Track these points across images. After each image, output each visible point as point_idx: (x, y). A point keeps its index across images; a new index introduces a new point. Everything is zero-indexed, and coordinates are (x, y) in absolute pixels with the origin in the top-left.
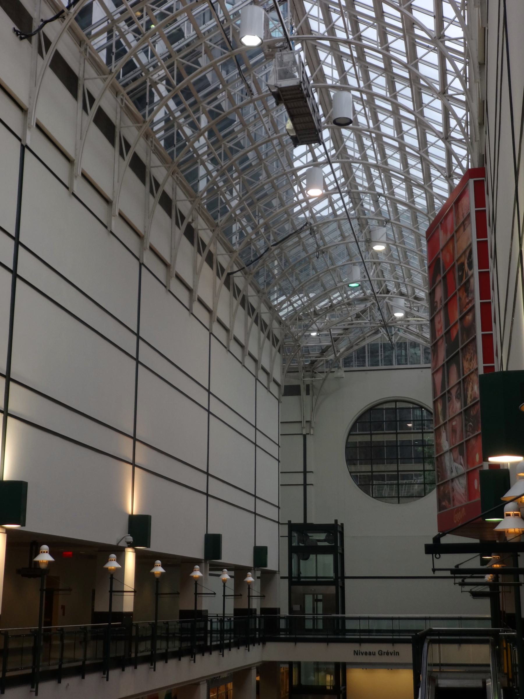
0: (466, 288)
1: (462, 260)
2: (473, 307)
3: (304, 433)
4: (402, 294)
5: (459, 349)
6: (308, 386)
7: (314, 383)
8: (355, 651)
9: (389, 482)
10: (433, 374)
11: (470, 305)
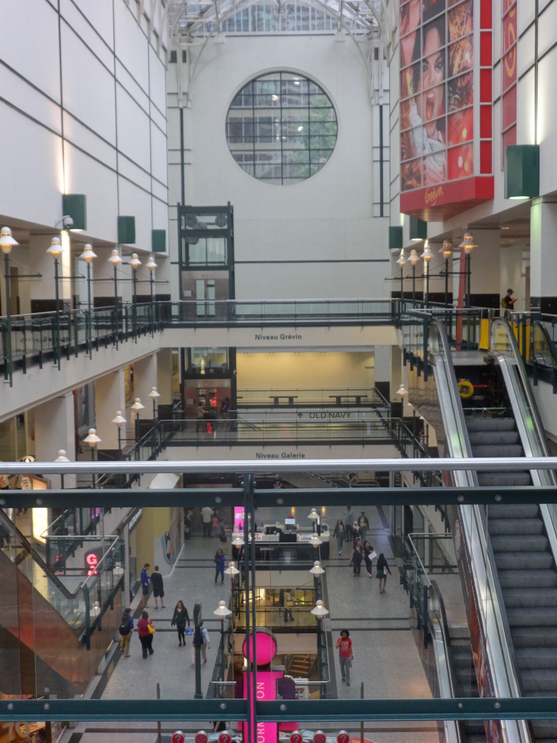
3: (181, 106)
5: (445, 11)
6: (184, 53)
7: (191, 50)
8: (256, 336)
9: (246, 162)
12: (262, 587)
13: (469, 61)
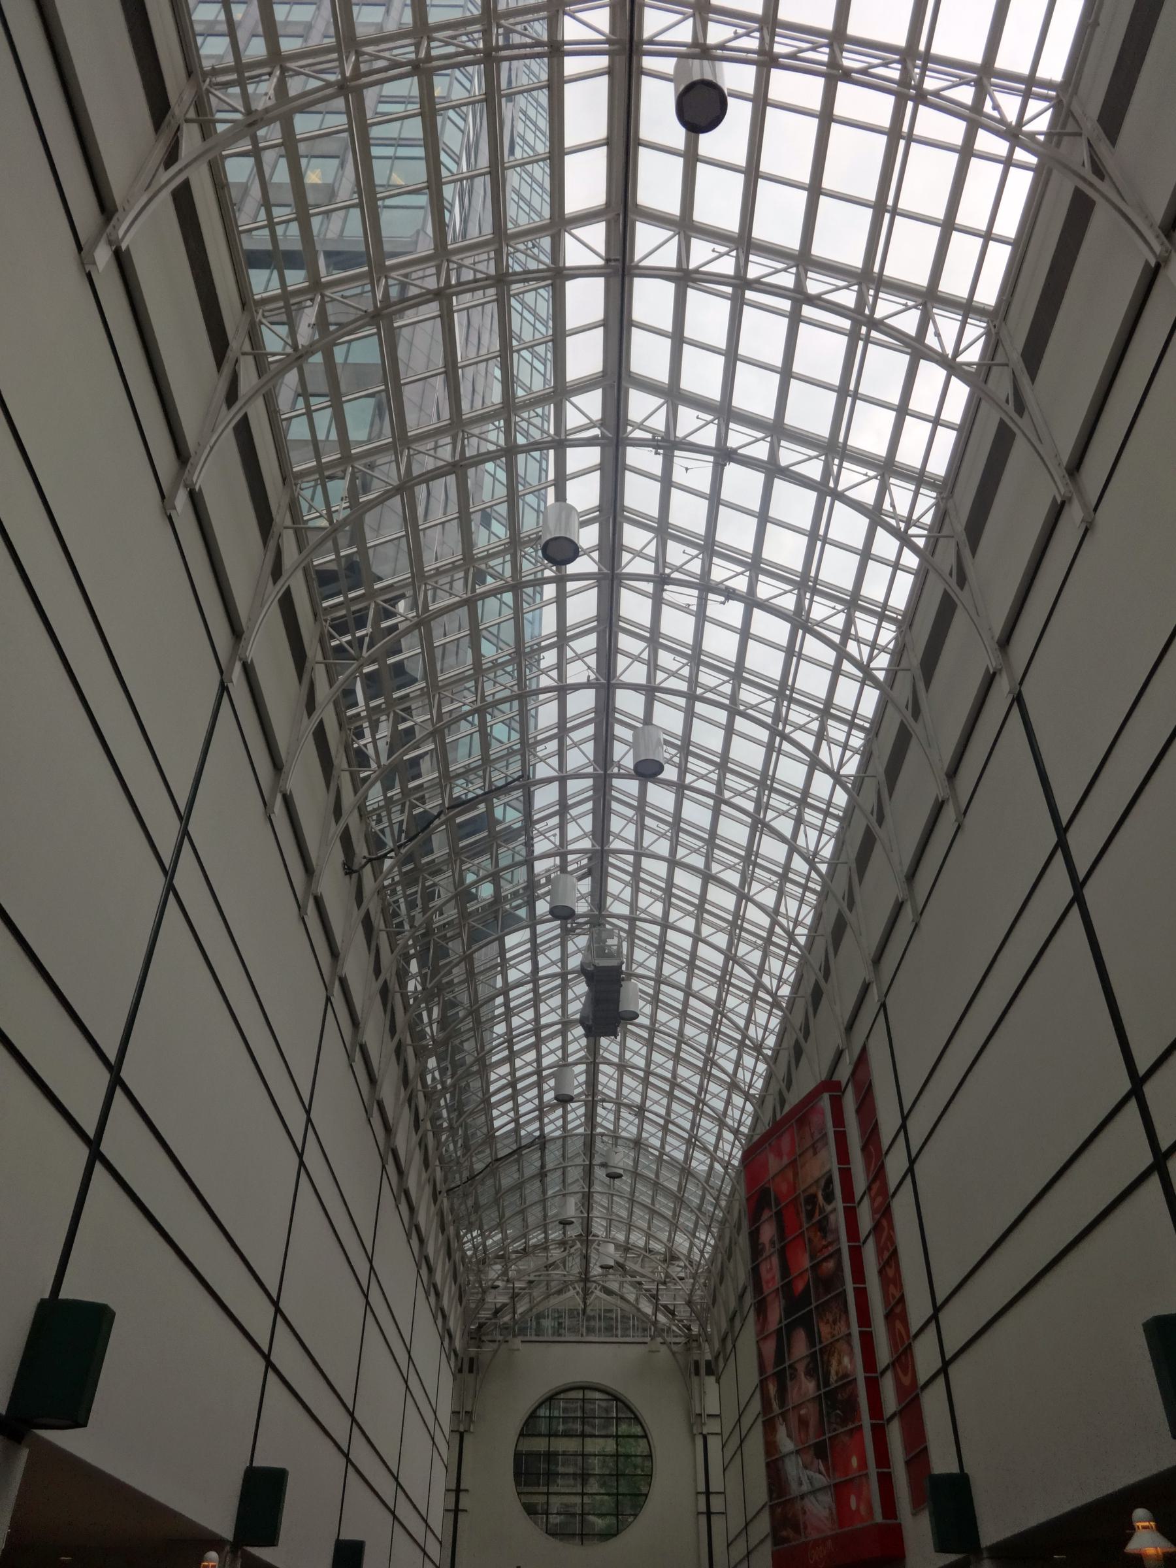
0: (823, 1227)
1: (812, 1191)
2: (839, 1250)
3: (462, 1429)
5: (813, 1306)
6: (471, 1360)
10: (757, 1342)
11: (831, 1249)
13: (849, 1366)
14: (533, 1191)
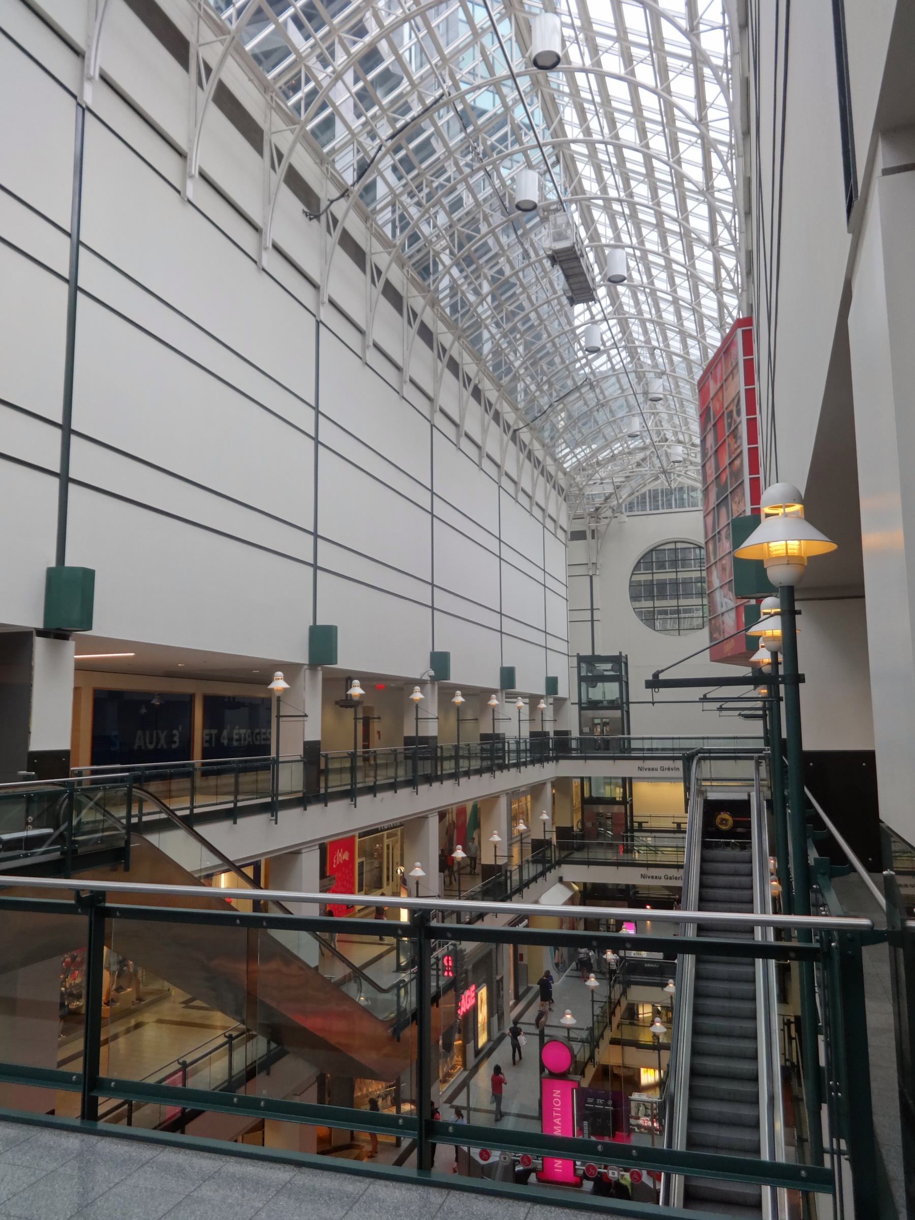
0: (734, 434)
2: (741, 452)
4: (679, 442)
6: (593, 531)
10: (705, 517)
11: (739, 451)
12: (648, 1003)
14: (602, 416)
